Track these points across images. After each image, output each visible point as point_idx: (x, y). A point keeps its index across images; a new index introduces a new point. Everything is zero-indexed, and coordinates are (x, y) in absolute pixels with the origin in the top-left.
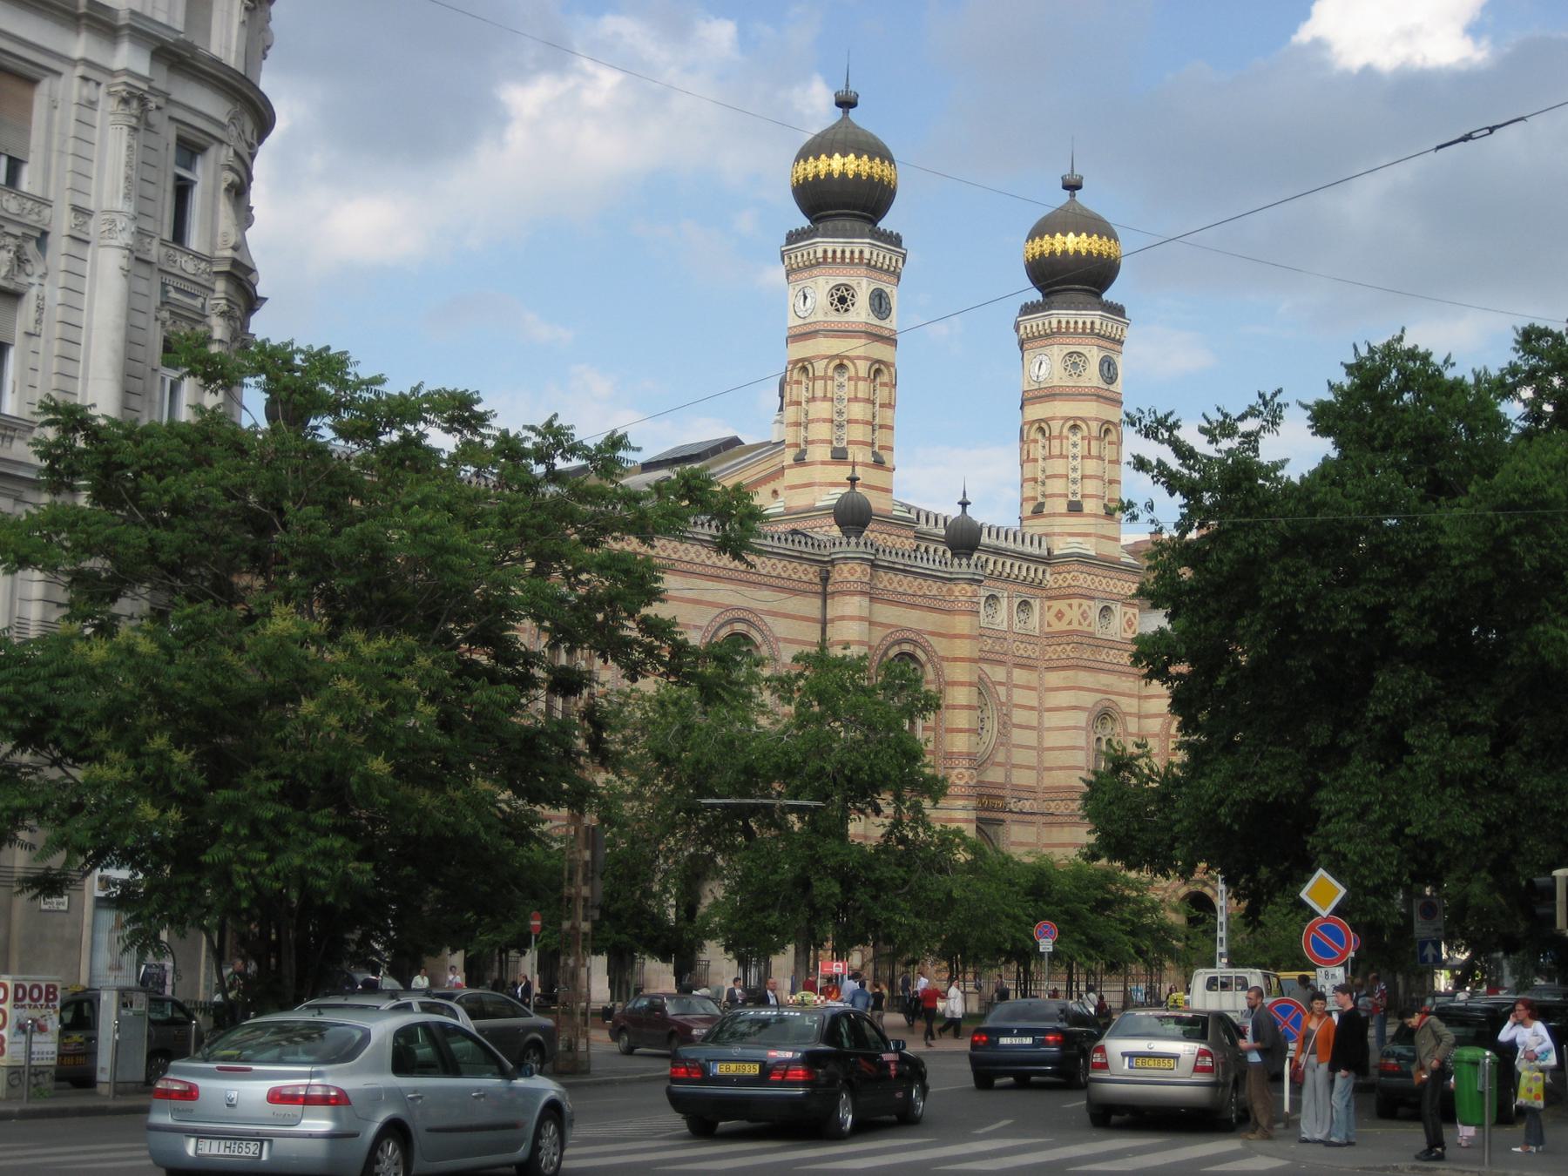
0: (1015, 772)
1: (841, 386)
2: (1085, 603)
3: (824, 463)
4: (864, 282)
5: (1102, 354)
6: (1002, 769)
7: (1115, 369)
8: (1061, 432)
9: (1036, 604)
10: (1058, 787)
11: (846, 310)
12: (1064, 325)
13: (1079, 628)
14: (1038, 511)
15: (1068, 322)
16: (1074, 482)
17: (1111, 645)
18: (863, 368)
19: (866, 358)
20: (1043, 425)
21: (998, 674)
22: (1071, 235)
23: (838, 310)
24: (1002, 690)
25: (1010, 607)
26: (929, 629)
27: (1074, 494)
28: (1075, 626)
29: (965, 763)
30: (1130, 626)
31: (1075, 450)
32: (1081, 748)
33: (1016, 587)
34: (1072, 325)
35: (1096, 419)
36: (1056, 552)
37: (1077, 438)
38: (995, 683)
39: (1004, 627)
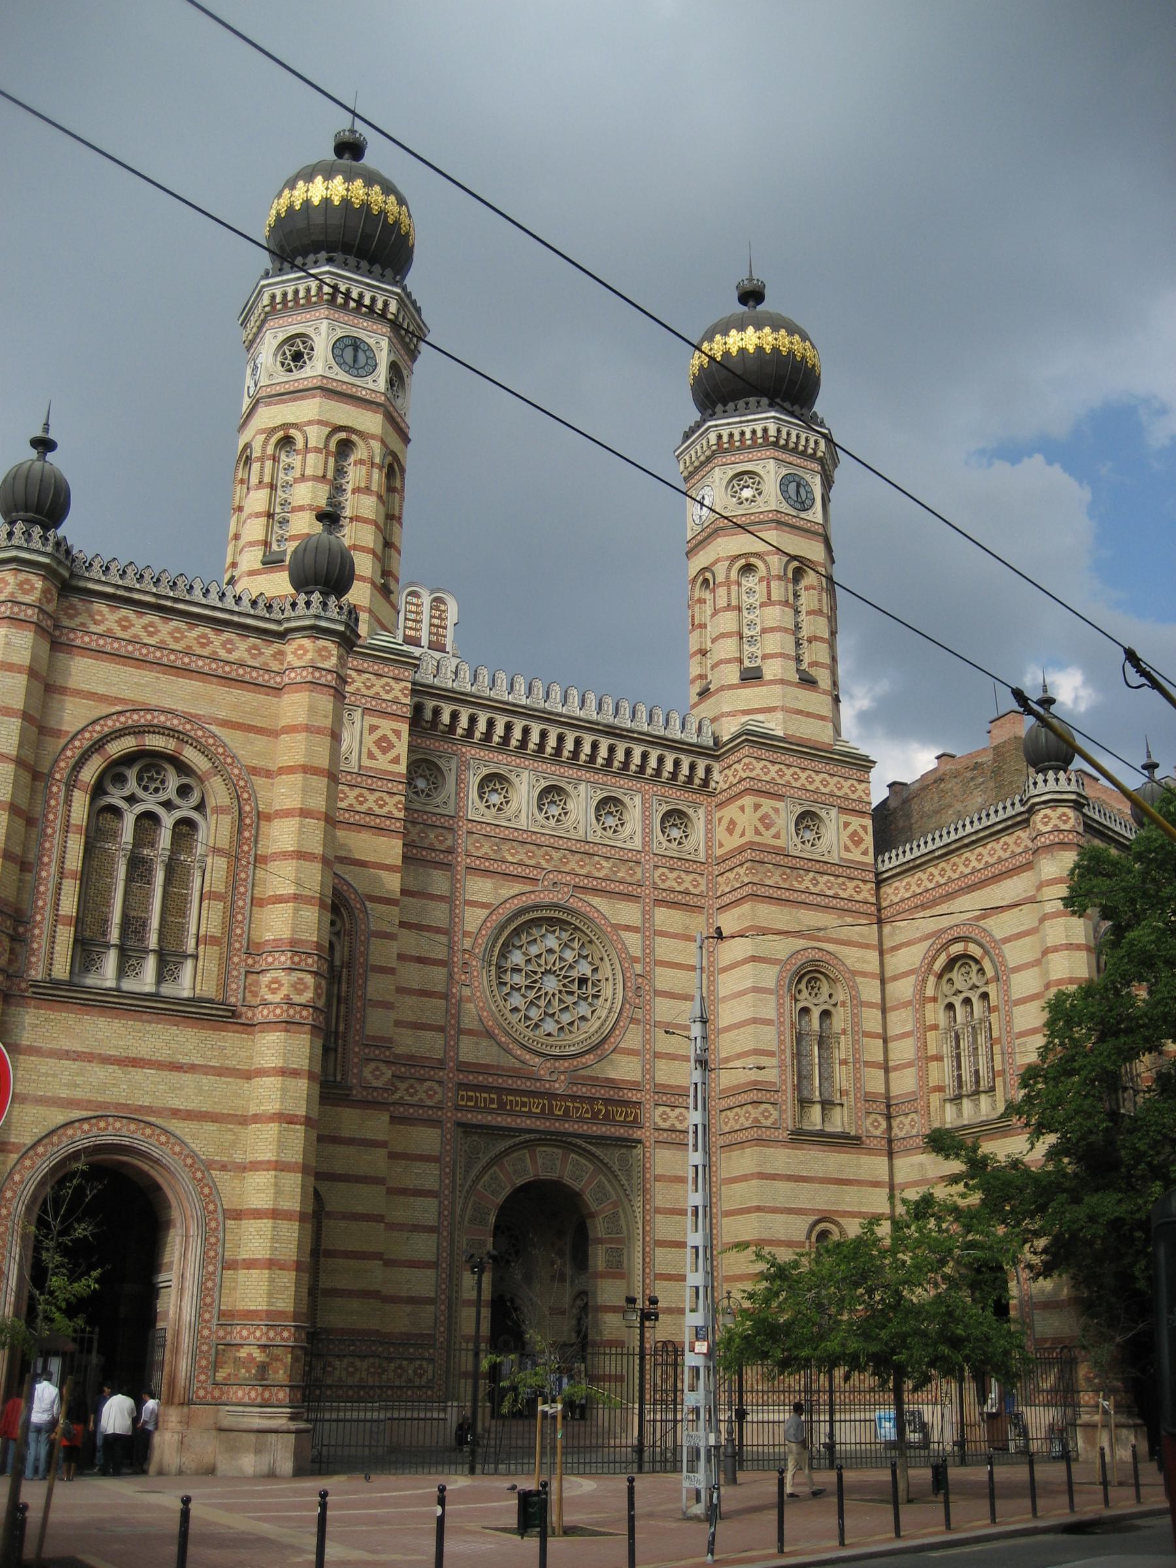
0: (661, 1064)
1: (289, 468)
2: (767, 804)
3: (252, 573)
4: (324, 326)
6: (635, 1059)
8: (728, 576)
9: (699, 819)
10: (738, 1086)
11: (302, 367)
12: (725, 439)
13: (757, 839)
14: (704, 693)
15: (731, 435)
16: (752, 640)
17: (822, 867)
18: (315, 436)
19: (320, 422)
20: (708, 575)
21: (629, 913)
22: (733, 332)
23: (290, 371)
24: (633, 942)
25: (646, 817)
26: (222, 714)
28: (750, 836)
29: (284, 959)
30: (857, 843)
32: (768, 1022)
33: (657, 789)
34: (737, 437)
36: (725, 739)
37: (750, 582)
39: (637, 844)
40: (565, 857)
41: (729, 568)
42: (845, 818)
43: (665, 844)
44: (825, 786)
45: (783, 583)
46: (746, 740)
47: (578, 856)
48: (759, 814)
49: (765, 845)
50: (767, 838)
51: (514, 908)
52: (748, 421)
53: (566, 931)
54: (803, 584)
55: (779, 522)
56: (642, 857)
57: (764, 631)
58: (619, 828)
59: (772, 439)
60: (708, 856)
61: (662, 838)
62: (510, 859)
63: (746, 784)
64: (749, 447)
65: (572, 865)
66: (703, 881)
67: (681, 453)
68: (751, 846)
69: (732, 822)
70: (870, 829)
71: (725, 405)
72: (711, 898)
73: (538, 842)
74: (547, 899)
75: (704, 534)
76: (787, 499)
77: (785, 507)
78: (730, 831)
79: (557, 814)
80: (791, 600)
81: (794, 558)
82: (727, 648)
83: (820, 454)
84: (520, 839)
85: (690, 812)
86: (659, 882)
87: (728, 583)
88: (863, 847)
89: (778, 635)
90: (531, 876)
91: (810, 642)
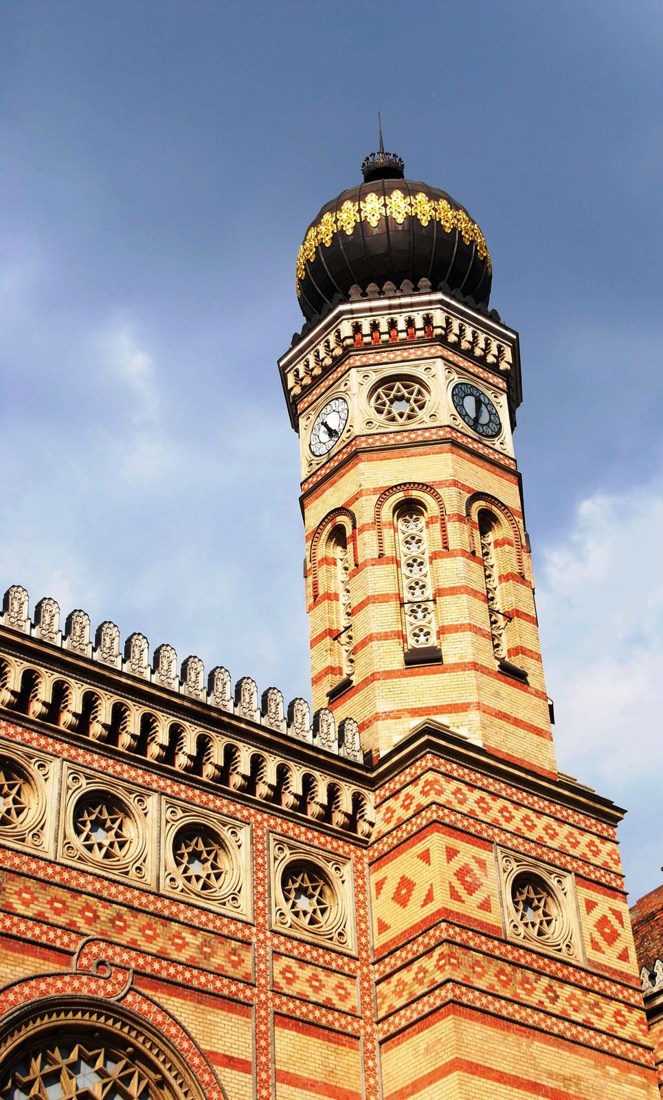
2: (468, 852)
5: (456, 379)
7: (494, 414)
9: (344, 880)
13: (455, 906)
14: (340, 692)
20: (342, 519)
25: (258, 868)
27: (420, 631)
28: (442, 900)
30: (612, 938)
31: (414, 550)
35: (455, 483)
36: (383, 753)
38: (210, 1058)
39: (245, 909)
40: (119, 917)
41: (380, 504)
42: (587, 893)
43: (290, 917)
44: (552, 837)
45: (466, 527)
46: (429, 744)
47: (143, 919)
48: (456, 864)
49: (469, 919)
50: (469, 906)
51: (22, 1001)
52: (401, 306)
53: (116, 1060)
54: (491, 537)
55: (454, 443)
56: (253, 934)
57: (439, 593)
58: (213, 881)
59: (438, 331)
60: (362, 947)
61: (286, 907)
62: (20, 909)
63: (431, 814)
64: (404, 343)
65: (132, 934)
66: (354, 989)
67: (290, 362)
68: (445, 916)
69: (406, 884)
70: (627, 918)
71: (364, 287)
72: (368, 1022)
73: (73, 884)
74: (85, 992)
75: (333, 464)
76: (464, 416)
77: (460, 424)
78: (401, 899)
79: (106, 843)
80: (479, 554)
81: (477, 496)
82: (381, 618)
83: (503, 366)
84: (41, 875)
85: (330, 869)
86: (282, 983)
87: (377, 523)
88: (619, 945)
89: (464, 598)
90: (58, 944)
91: (508, 617)
